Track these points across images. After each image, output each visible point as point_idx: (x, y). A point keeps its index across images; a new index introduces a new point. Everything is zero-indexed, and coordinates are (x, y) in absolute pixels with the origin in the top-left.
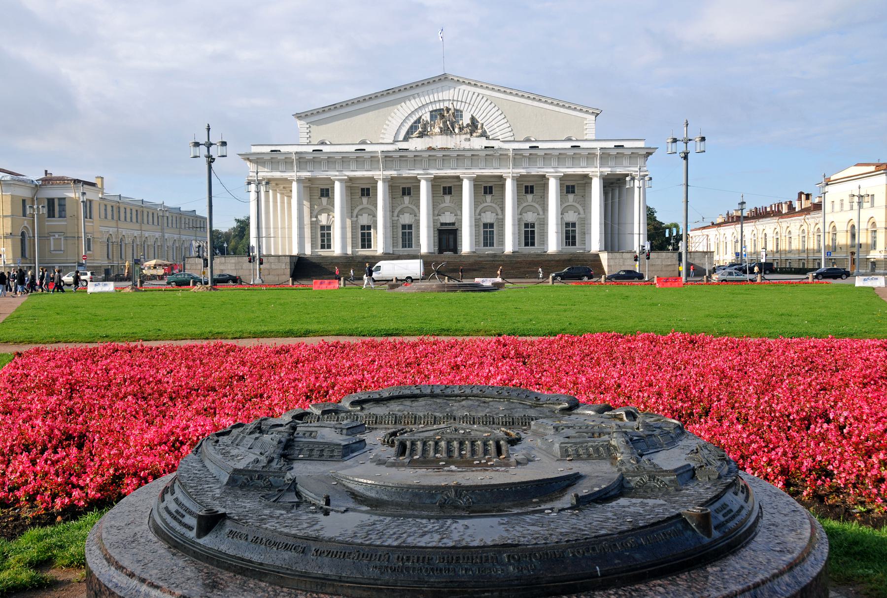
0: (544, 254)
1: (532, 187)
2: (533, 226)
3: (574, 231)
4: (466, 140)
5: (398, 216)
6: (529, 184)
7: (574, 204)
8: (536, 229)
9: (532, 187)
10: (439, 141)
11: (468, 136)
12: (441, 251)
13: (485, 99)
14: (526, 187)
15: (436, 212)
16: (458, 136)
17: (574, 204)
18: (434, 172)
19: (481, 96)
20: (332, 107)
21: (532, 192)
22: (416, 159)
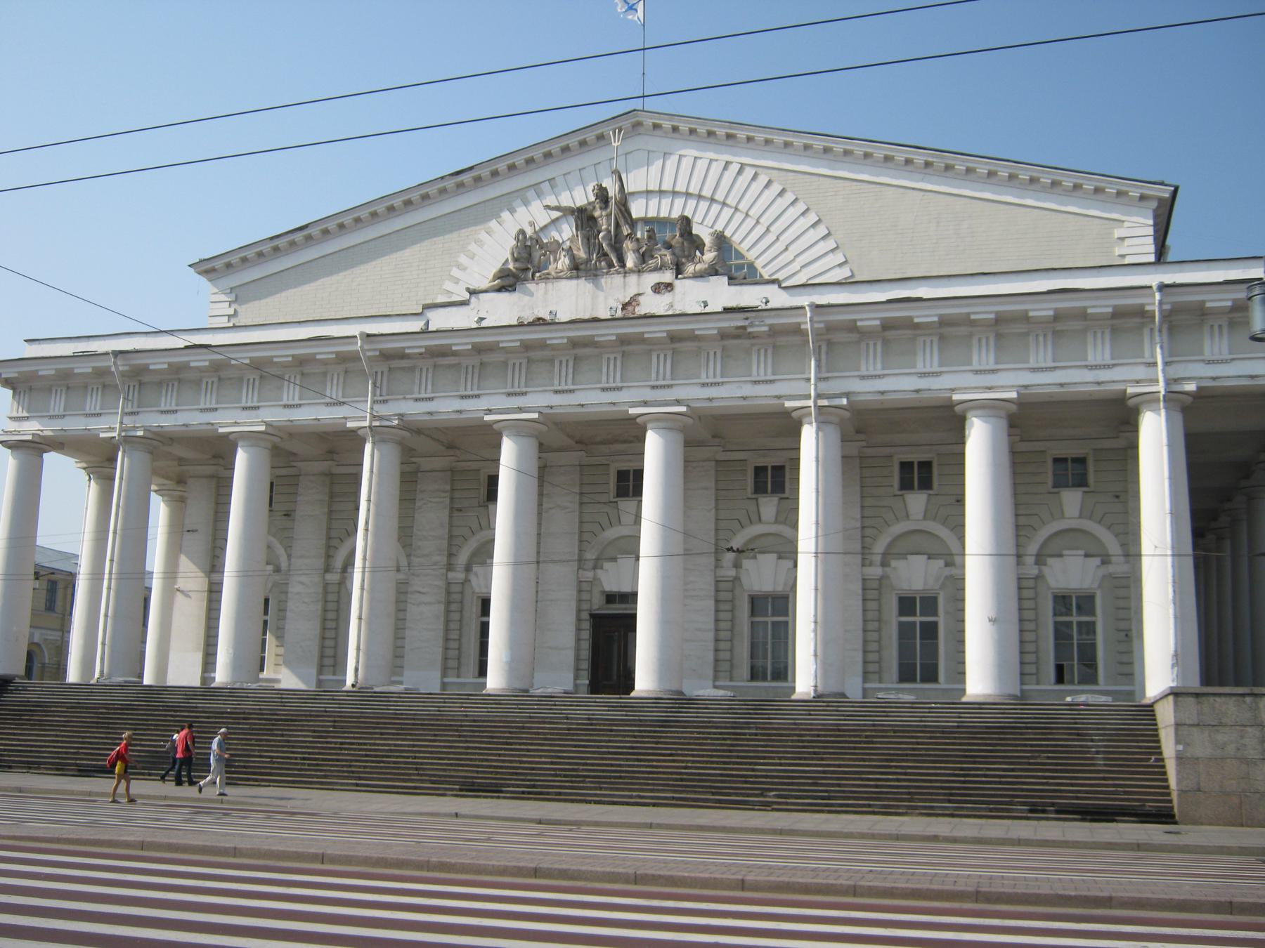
0: (957, 705)
1: (926, 466)
2: (930, 604)
3: (1089, 628)
4: (658, 288)
5: (468, 569)
6: (915, 457)
7: (1088, 525)
8: (941, 620)
9: (926, 466)
10: (565, 299)
11: (667, 276)
12: (595, 688)
13: (763, 179)
14: (906, 467)
15: (590, 555)
16: (633, 279)
17: (1088, 525)
18: (541, 400)
19: (749, 172)
20: (299, 237)
21: (926, 484)
22: (482, 356)
